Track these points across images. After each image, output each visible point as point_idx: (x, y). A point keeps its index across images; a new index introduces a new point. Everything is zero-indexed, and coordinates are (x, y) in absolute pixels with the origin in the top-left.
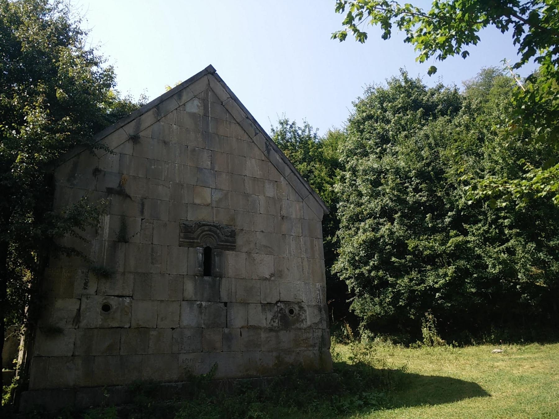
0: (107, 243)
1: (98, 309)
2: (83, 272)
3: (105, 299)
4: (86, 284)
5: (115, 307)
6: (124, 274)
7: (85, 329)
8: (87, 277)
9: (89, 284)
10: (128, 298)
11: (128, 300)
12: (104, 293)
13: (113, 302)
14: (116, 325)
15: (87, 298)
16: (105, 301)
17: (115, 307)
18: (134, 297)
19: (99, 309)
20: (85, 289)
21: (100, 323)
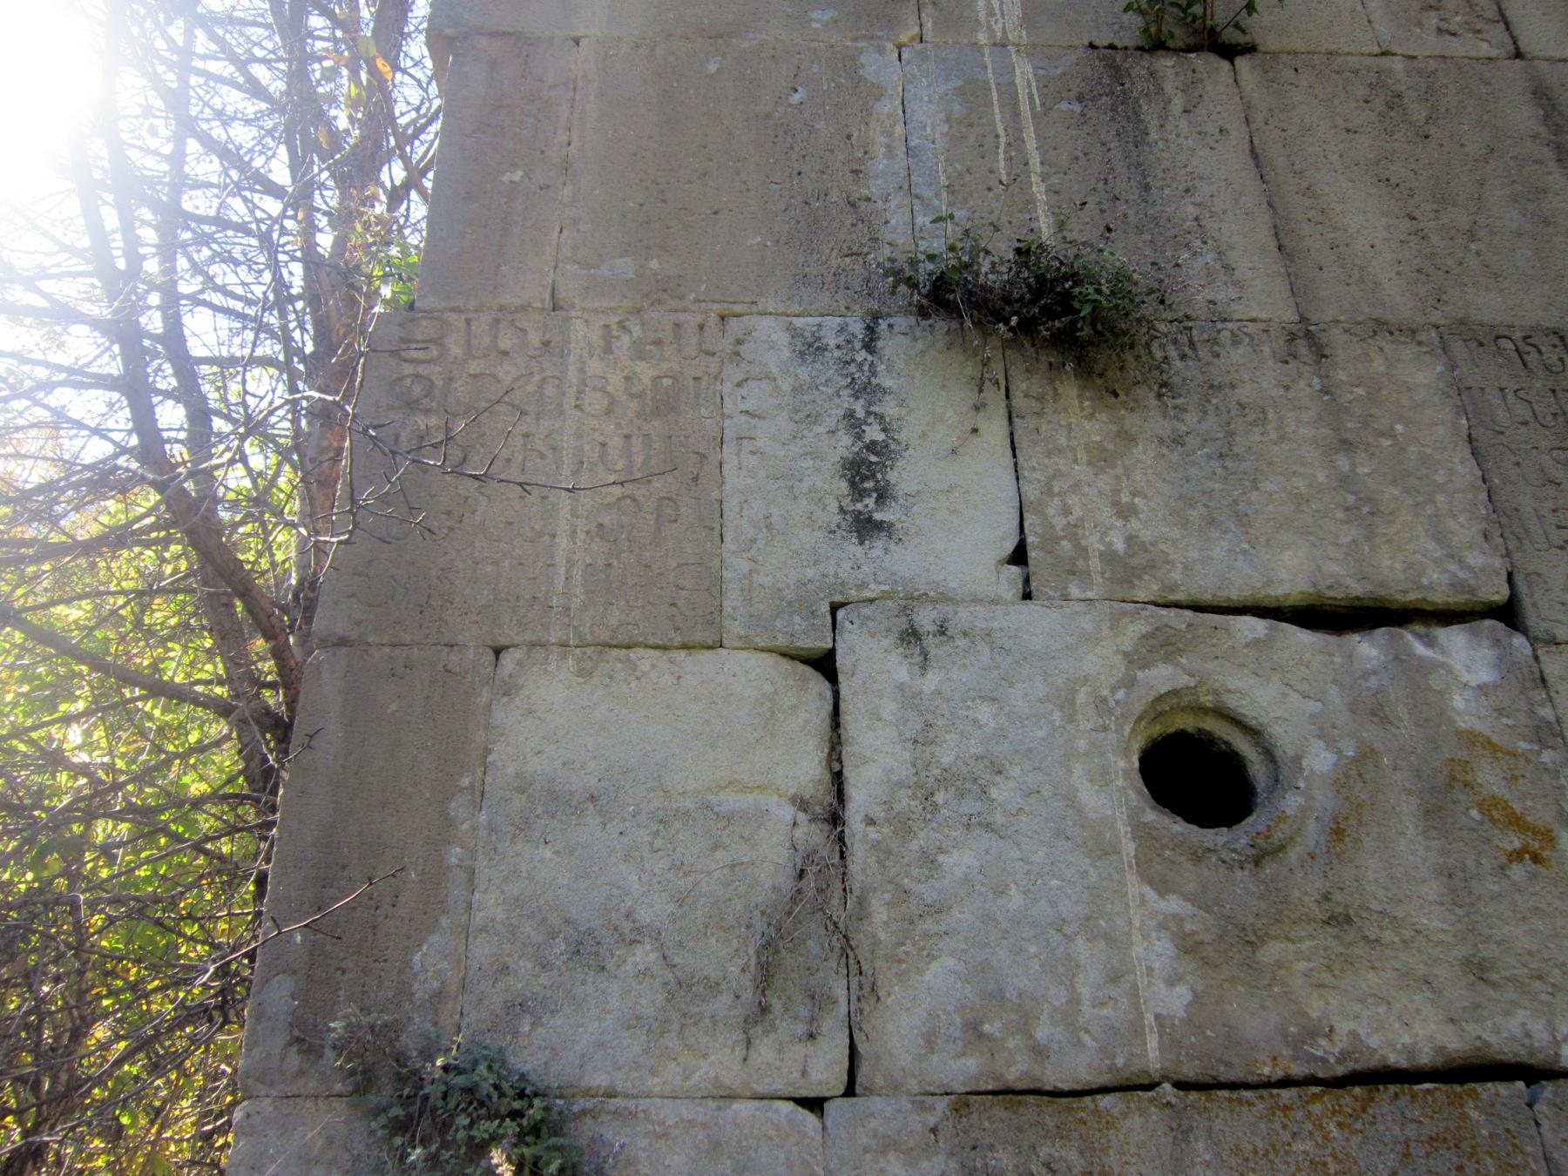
0: (1023, 71)
1: (1088, 796)
2: (811, 348)
3: (1161, 646)
4: (866, 473)
5: (1320, 760)
6: (1306, 340)
7: (963, 1101)
8: (866, 390)
9: (902, 477)
10: (1454, 639)
11: (1466, 657)
12: (1125, 568)
13: (1283, 693)
14: (1416, 1030)
15: (911, 636)
16: (1162, 677)
17: (1320, 760)
18: (1539, 610)
19: (1113, 794)
20: (866, 527)
21: (1175, 1001)
